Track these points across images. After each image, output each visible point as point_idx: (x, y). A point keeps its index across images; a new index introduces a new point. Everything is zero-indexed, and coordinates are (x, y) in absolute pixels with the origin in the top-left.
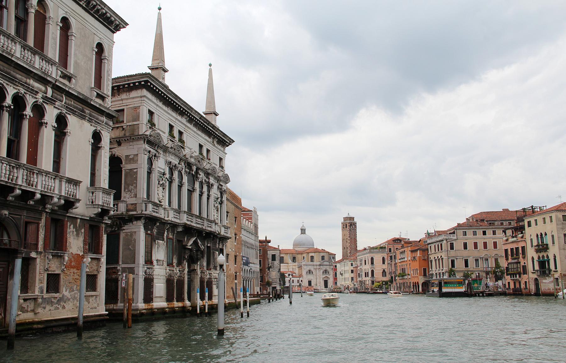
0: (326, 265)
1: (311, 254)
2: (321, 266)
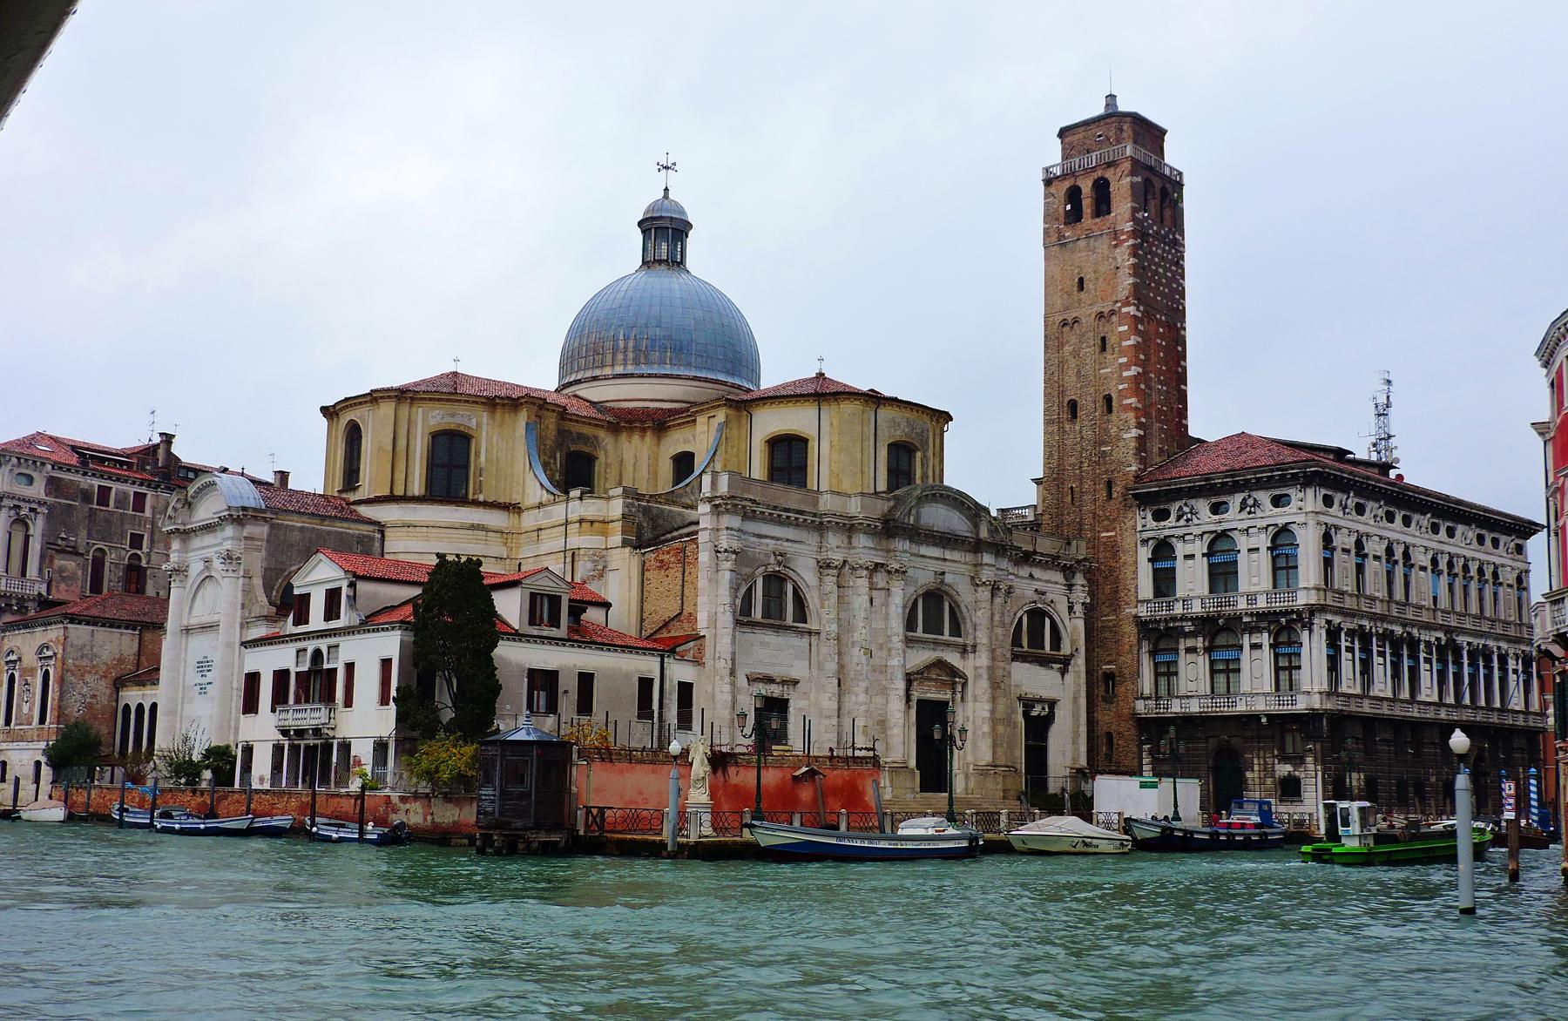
0: (946, 540)
1: (769, 422)
2: (902, 545)
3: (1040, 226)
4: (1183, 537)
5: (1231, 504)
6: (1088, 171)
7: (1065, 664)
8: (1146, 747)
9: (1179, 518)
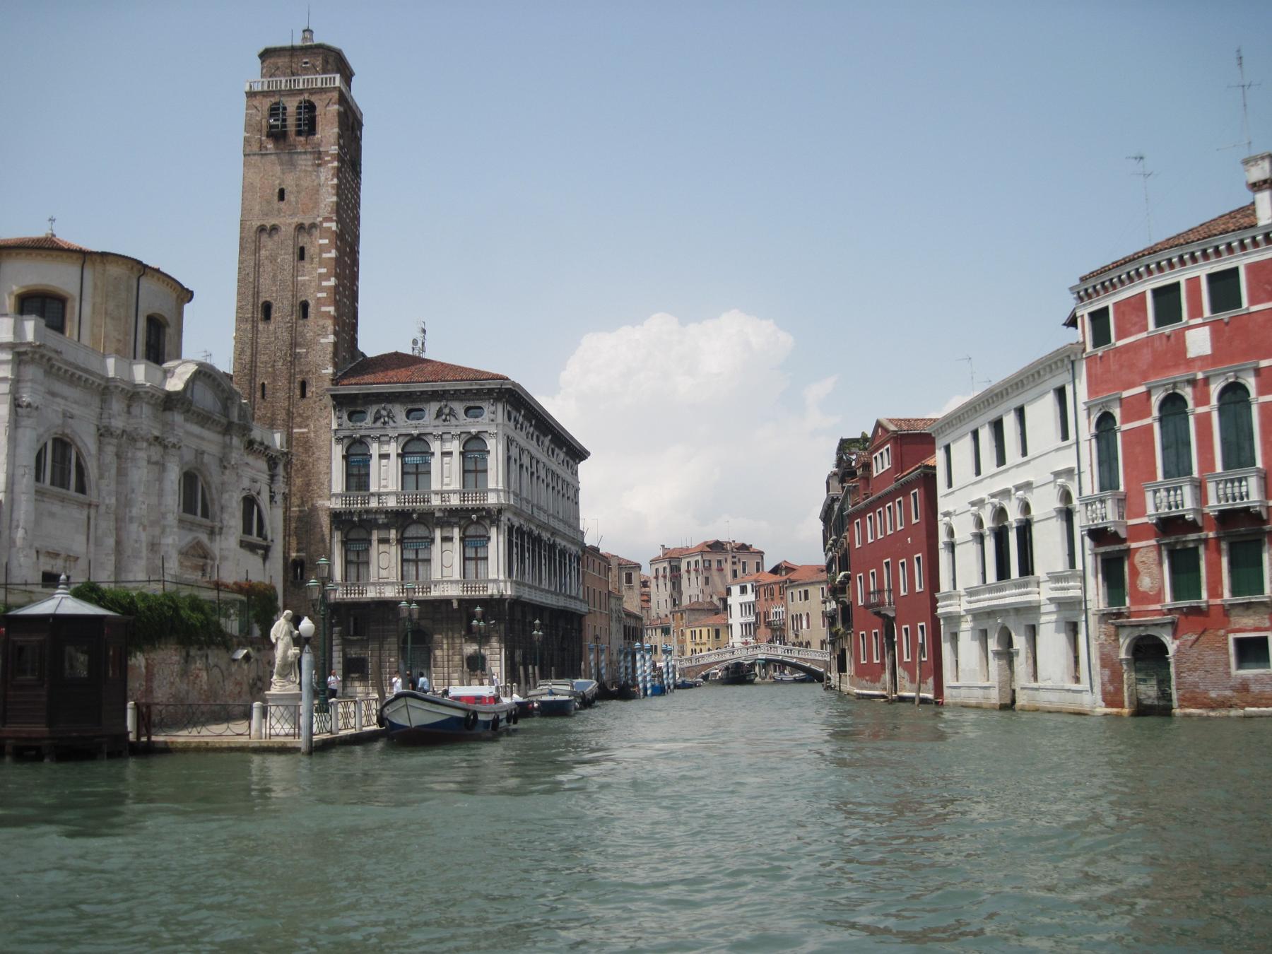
2: (178, 418)
3: (242, 134)
4: (379, 438)
5: (427, 412)
6: (292, 93)
7: (267, 549)
8: (336, 629)
9: (376, 420)
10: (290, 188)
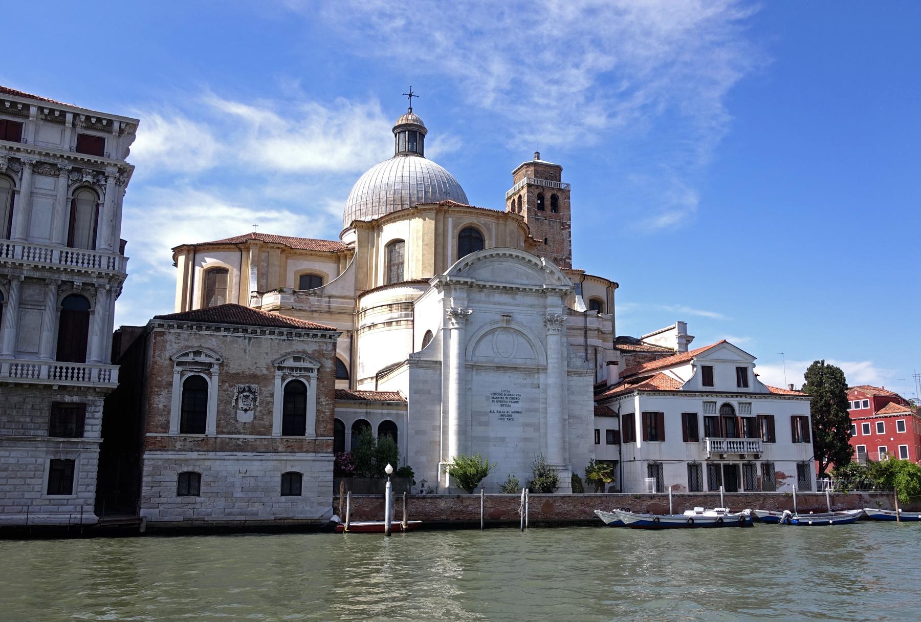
10: (550, 239)
